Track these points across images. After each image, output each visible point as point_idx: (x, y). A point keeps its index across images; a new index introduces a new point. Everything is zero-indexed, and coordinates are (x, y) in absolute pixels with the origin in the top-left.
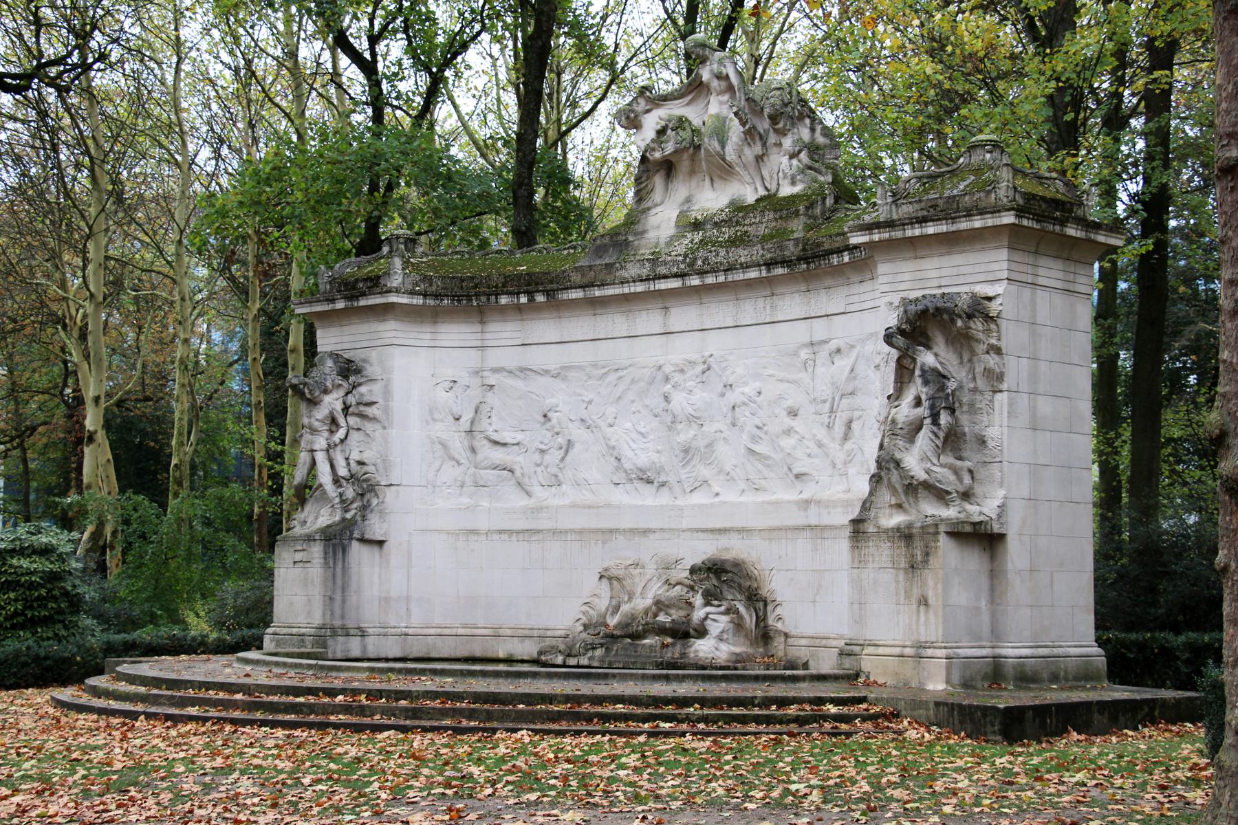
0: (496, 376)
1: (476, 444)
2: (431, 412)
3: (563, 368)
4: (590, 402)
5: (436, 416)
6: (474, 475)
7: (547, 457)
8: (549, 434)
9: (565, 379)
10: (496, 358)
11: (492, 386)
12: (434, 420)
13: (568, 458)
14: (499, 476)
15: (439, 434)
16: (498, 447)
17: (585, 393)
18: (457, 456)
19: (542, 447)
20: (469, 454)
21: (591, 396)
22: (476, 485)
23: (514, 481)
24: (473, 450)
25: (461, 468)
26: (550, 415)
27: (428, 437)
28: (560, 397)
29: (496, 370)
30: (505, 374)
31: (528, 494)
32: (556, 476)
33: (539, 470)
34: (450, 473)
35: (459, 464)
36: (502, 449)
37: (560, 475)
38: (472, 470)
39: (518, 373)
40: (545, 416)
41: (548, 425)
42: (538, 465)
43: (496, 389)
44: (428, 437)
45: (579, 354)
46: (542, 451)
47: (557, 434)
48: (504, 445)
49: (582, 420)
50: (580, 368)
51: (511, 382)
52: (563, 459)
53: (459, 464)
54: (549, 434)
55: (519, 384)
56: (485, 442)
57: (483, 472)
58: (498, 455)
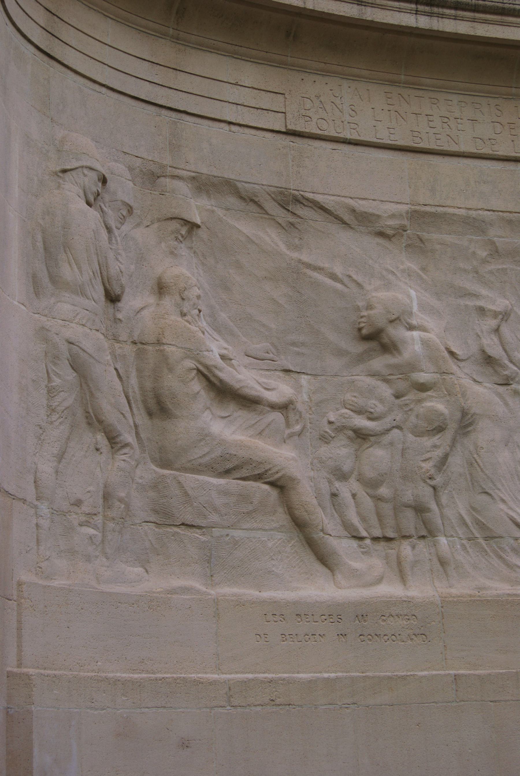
0: (204, 202)
1: (170, 382)
2: (49, 254)
3: (417, 216)
4: (505, 316)
5: (67, 272)
6: (157, 485)
7: (378, 456)
8: (386, 391)
9: (418, 247)
10: (209, 149)
11: (193, 226)
12: (54, 280)
13: (457, 463)
14: (244, 497)
15: (74, 332)
16: (232, 408)
17: (484, 292)
18: (111, 416)
19: (361, 422)
20: (142, 419)
21: (500, 304)
22: (163, 516)
23: (281, 517)
24: (159, 408)
25: (121, 460)
26: (398, 333)
27: (43, 334)
28: (398, 288)
29: (203, 185)
30: (232, 201)
31: (324, 558)
32: (420, 509)
33: (345, 490)
34: (90, 469)
35: (113, 440)
36: (242, 416)
37: (433, 506)
38: (148, 471)
39: (271, 206)
40: (375, 339)
41: (379, 363)
42: (343, 477)
43: (202, 233)
44: (43, 334)
45: (455, 187)
46: (361, 436)
47: (423, 387)
48: (248, 402)
49: (488, 360)
50: (474, 225)
51: (246, 227)
52: (444, 460)
53: (113, 440)
54: (386, 391)
55: (271, 238)
56: (197, 386)
57: (190, 479)
58: (228, 430)
